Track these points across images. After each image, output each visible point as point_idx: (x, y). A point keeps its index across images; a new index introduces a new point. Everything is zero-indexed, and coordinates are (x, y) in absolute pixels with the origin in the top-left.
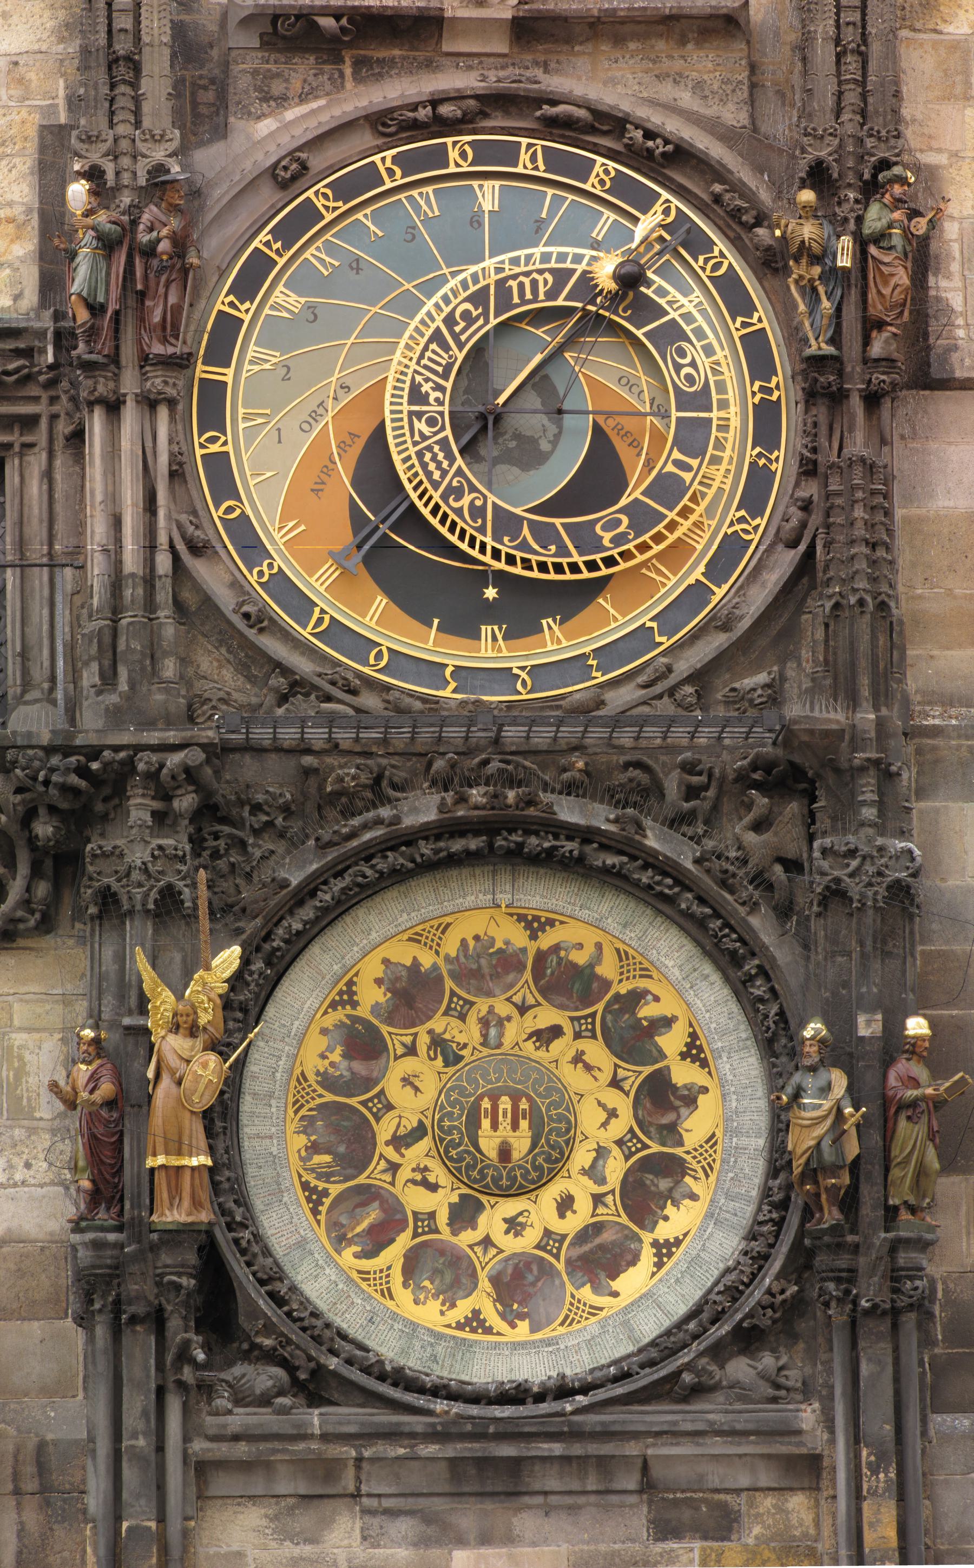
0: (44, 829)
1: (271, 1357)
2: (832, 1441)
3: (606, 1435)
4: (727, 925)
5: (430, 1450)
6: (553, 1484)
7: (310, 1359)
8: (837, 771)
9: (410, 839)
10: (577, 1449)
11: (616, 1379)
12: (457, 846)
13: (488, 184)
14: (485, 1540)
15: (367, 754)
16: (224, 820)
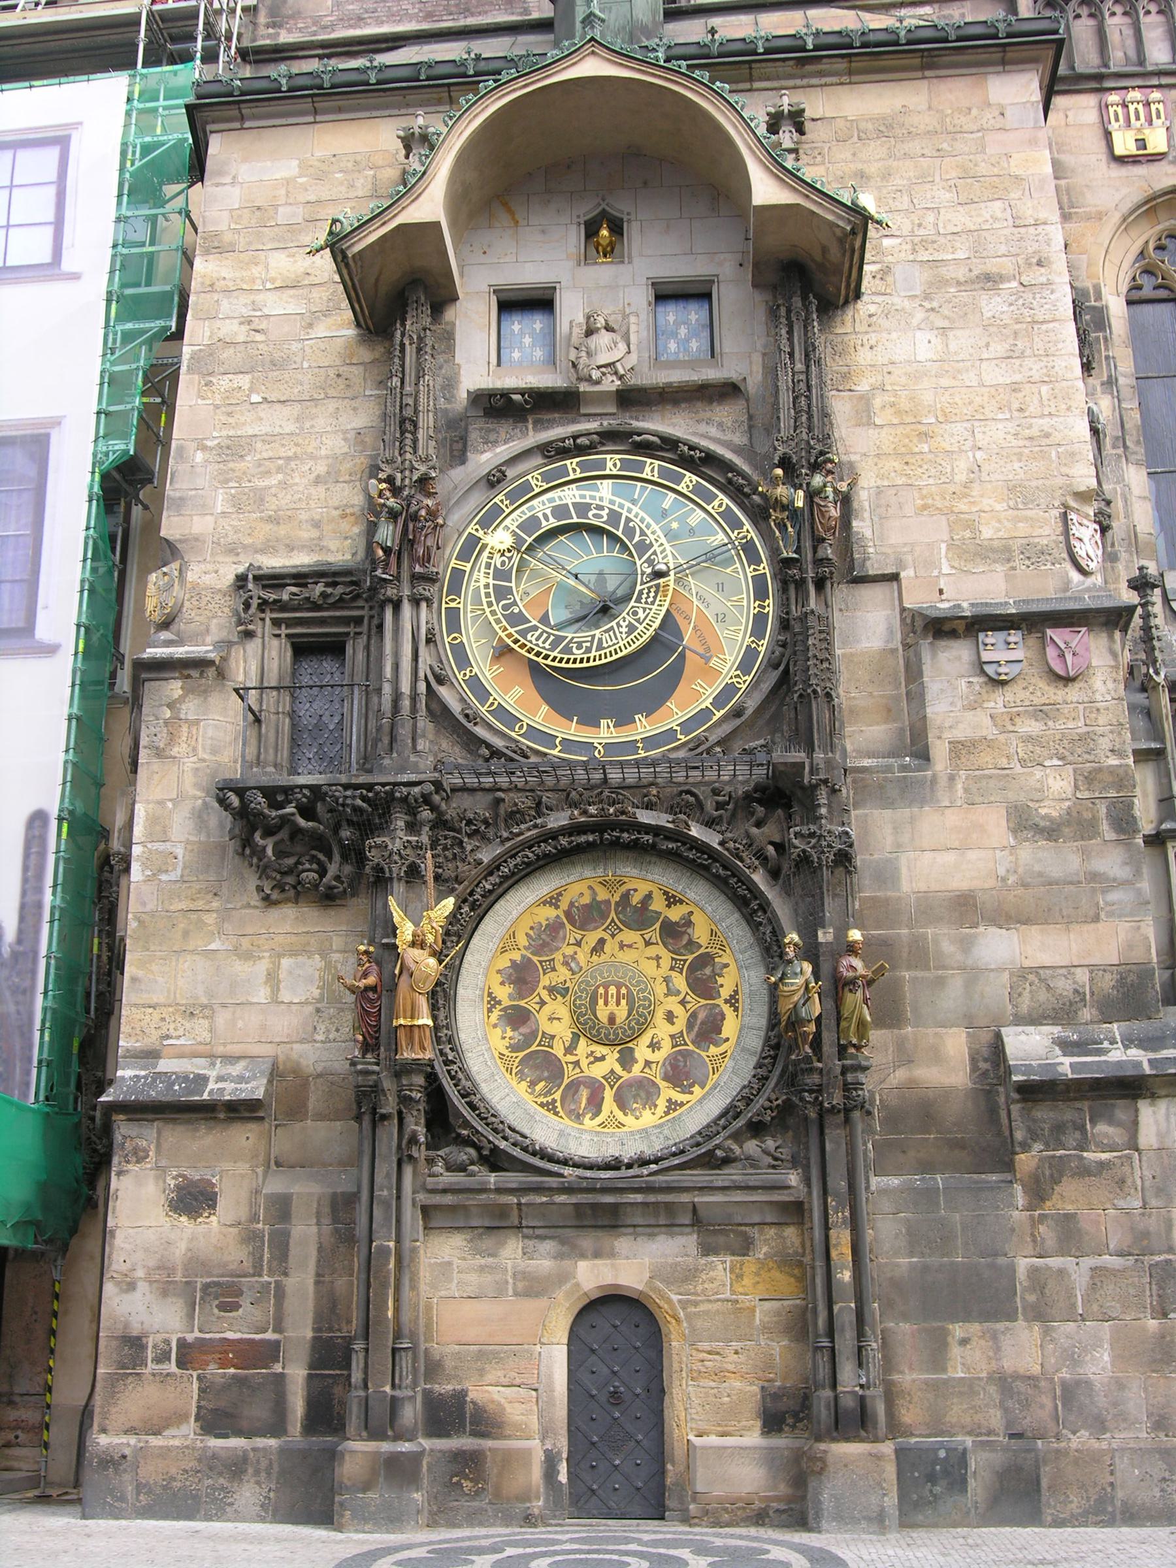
0: (346, 833)
1: (468, 1142)
2: (810, 1193)
3: (669, 1189)
4: (739, 881)
5: (561, 1198)
6: (639, 1221)
7: (490, 1142)
8: (803, 788)
9: (553, 835)
10: (651, 1198)
11: (674, 1155)
12: (582, 839)
13: (605, 482)
14: (597, 1255)
15: (532, 791)
16: (453, 830)
